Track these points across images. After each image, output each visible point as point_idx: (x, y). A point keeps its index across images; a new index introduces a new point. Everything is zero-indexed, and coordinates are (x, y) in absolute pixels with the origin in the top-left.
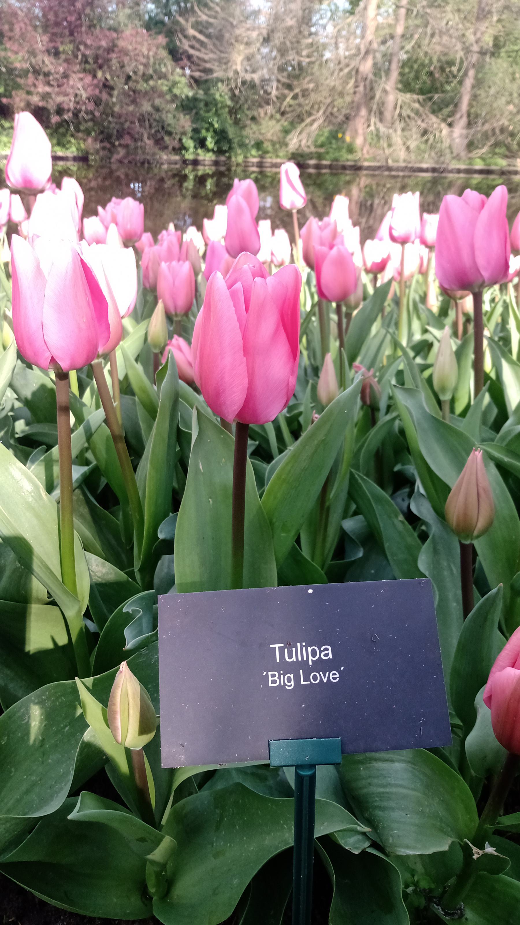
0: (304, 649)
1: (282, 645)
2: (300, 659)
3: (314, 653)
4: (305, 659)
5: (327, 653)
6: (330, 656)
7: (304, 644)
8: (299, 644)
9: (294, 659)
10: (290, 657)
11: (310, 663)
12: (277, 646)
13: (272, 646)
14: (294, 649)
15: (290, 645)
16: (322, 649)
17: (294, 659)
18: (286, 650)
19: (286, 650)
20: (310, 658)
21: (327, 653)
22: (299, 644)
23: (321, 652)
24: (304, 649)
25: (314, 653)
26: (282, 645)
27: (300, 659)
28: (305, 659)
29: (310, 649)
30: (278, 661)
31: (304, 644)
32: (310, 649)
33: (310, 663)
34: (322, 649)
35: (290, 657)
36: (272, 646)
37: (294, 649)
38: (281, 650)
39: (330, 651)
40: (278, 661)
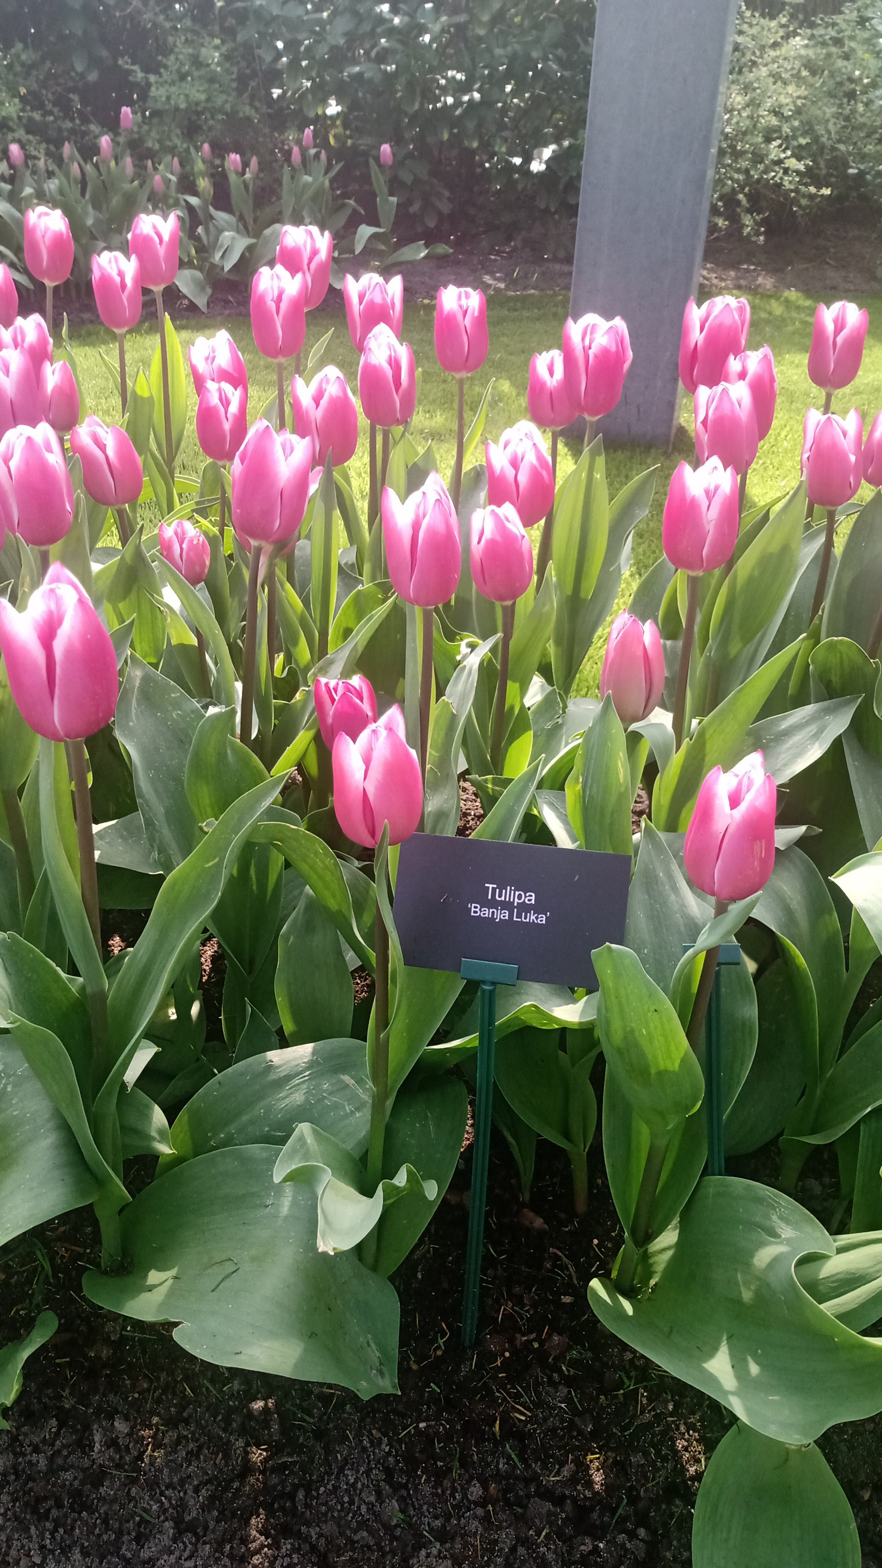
3: (520, 897)
5: (531, 898)
6: (533, 902)
9: (503, 898)
10: (500, 896)
12: (491, 886)
15: (502, 887)
17: (503, 898)
20: (516, 900)
21: (531, 898)
23: (526, 897)
25: (520, 897)
29: (517, 893)
32: (517, 893)
35: (500, 896)
38: (494, 889)
39: (533, 898)
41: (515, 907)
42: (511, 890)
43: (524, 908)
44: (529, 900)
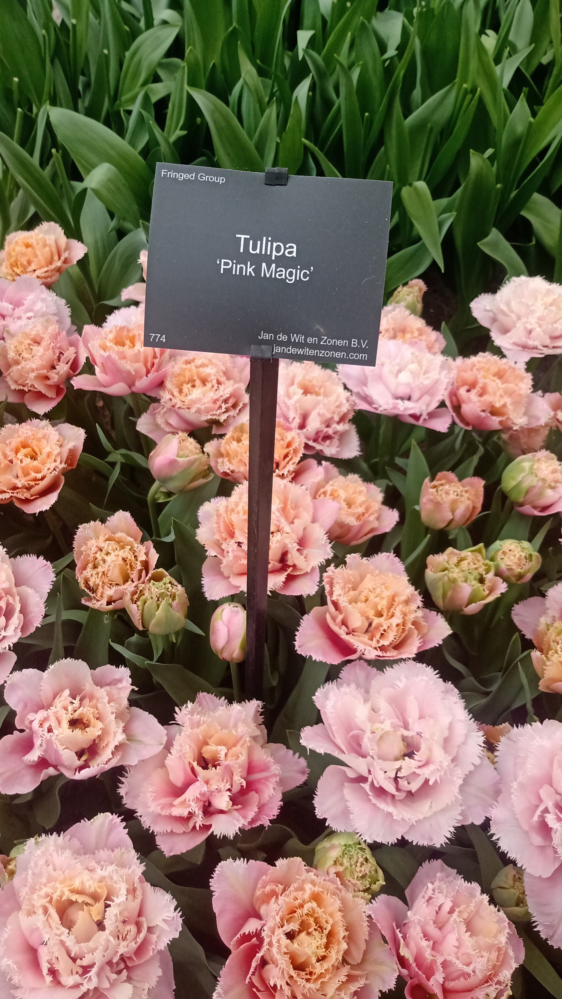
0: (269, 243)
1: (248, 237)
2: (263, 253)
3: (278, 249)
4: (269, 253)
5: (291, 251)
6: (294, 254)
7: (270, 239)
8: (265, 238)
9: (258, 251)
10: (254, 248)
11: (273, 258)
12: (243, 237)
13: (237, 236)
14: (259, 242)
15: (256, 238)
16: (287, 246)
18: (251, 242)
19: (251, 242)
20: (274, 253)
21: (291, 251)
22: (265, 238)
23: (285, 249)
24: (269, 243)
25: (278, 249)
26: (248, 237)
27: (263, 253)
28: (269, 253)
29: (275, 245)
30: (242, 251)
31: (270, 239)
32: (275, 245)
33: (273, 258)
34: (287, 246)
35: (254, 248)
36: (237, 236)
37: (259, 242)
38: (247, 241)
40: (242, 251)
41: (273, 262)
42: (267, 241)
43: (282, 262)
44: (289, 253)
